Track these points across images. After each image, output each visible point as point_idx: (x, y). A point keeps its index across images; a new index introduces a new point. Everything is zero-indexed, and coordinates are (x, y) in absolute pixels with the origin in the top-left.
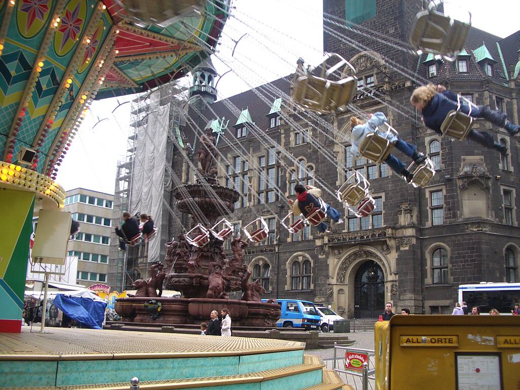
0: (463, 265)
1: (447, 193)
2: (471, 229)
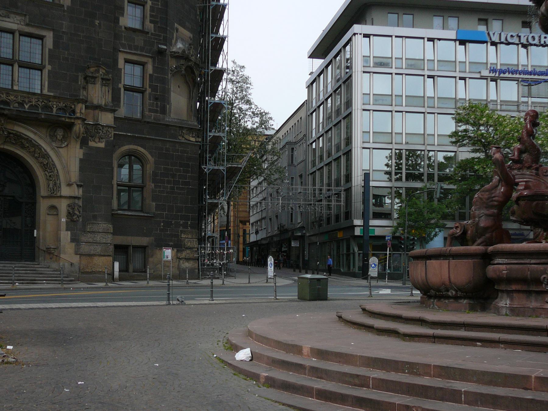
0: (172, 188)
1: (154, 71)
2: (187, 137)
